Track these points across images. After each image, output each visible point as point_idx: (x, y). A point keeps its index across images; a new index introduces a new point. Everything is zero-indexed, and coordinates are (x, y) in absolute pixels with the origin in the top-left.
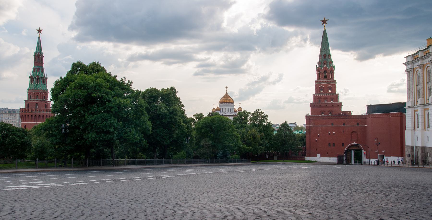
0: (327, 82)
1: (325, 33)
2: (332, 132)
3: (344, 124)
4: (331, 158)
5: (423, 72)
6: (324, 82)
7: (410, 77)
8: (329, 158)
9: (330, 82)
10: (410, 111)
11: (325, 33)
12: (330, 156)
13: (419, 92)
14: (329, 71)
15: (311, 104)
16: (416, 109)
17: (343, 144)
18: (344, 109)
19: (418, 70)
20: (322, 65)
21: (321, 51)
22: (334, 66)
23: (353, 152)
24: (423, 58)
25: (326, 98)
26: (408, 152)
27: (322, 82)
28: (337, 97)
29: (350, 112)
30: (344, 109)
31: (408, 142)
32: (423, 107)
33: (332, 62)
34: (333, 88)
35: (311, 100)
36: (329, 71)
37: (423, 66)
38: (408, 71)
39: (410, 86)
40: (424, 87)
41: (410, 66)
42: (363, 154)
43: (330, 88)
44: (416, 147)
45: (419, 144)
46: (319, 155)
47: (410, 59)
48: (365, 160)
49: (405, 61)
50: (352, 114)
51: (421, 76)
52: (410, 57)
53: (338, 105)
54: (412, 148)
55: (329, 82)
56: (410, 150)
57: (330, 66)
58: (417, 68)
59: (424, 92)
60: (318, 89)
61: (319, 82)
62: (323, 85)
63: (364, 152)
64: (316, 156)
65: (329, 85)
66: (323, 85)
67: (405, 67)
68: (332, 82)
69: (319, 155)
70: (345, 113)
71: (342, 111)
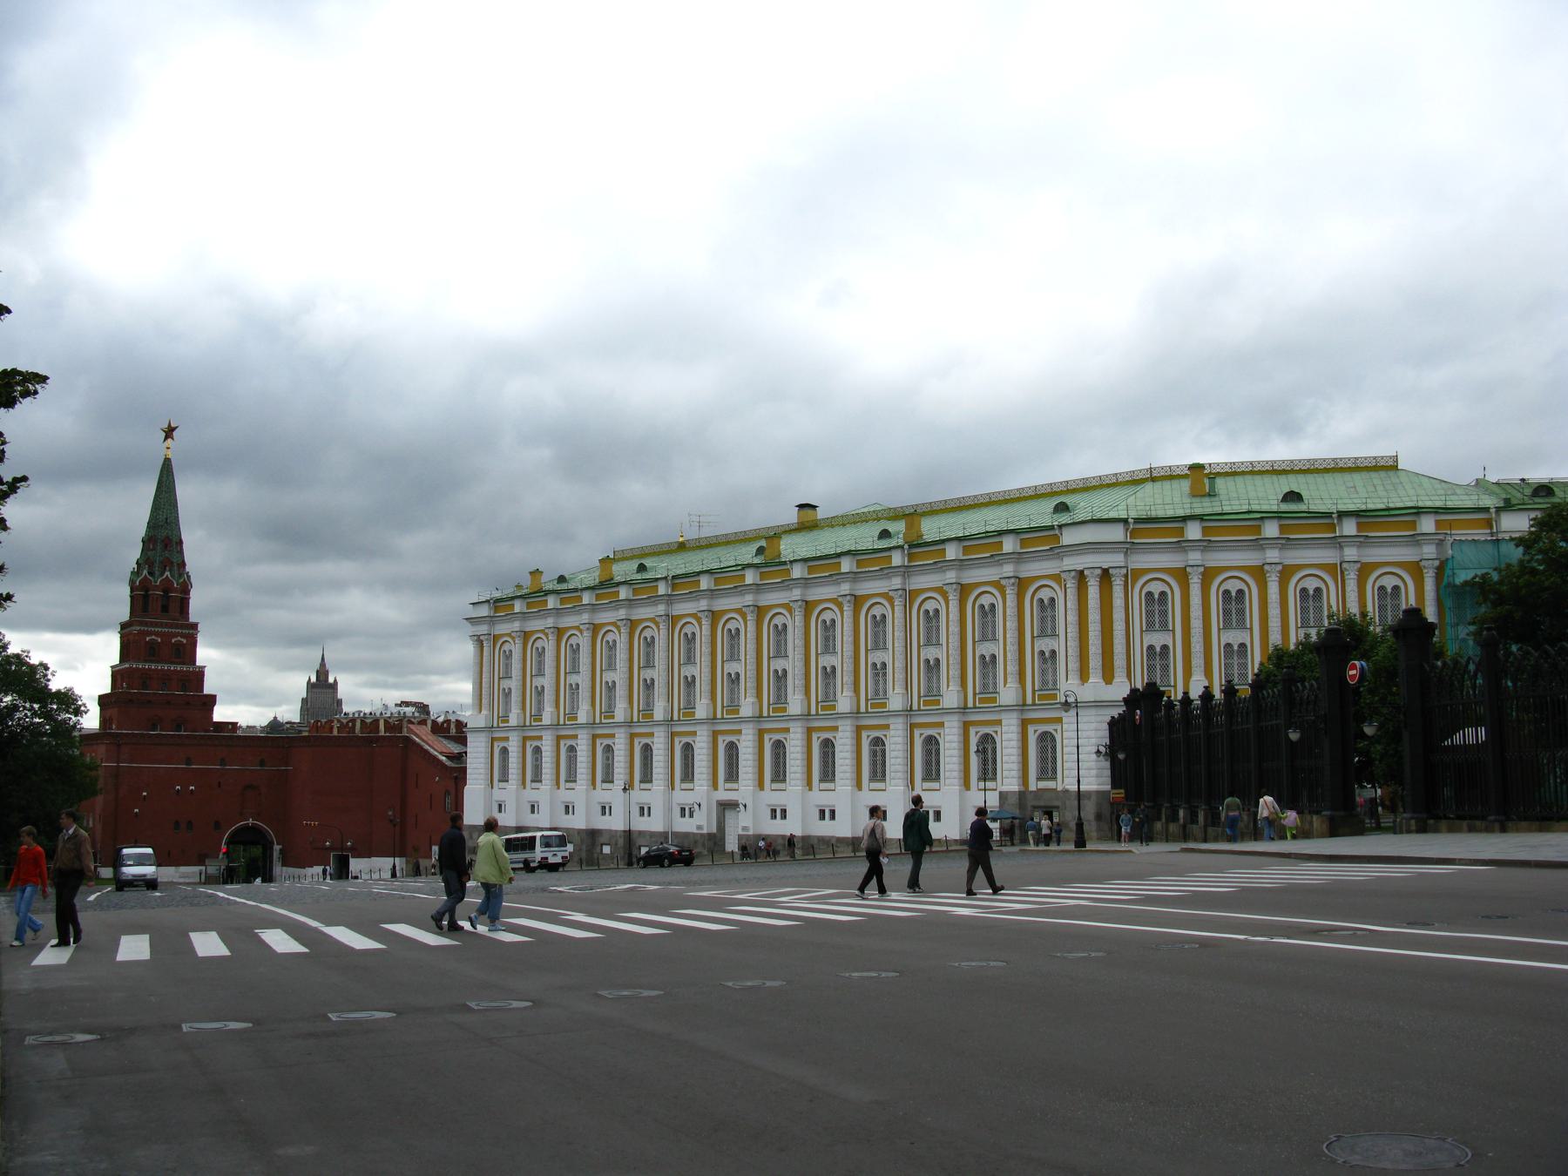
0: (171, 626)
3: (223, 762)
4: (183, 869)
6: (161, 625)
9: (177, 626)
12: (177, 863)
14: (175, 590)
17: (217, 825)
20: (157, 571)
21: (153, 525)
25: (165, 678)
27: (156, 625)
28: (199, 675)
29: (234, 724)
30: (220, 714)
33: (183, 564)
36: (175, 590)
42: (276, 854)
48: (278, 869)
57: (180, 575)
62: (157, 634)
63: (277, 848)
65: (176, 635)
66: (157, 634)
70: (222, 726)
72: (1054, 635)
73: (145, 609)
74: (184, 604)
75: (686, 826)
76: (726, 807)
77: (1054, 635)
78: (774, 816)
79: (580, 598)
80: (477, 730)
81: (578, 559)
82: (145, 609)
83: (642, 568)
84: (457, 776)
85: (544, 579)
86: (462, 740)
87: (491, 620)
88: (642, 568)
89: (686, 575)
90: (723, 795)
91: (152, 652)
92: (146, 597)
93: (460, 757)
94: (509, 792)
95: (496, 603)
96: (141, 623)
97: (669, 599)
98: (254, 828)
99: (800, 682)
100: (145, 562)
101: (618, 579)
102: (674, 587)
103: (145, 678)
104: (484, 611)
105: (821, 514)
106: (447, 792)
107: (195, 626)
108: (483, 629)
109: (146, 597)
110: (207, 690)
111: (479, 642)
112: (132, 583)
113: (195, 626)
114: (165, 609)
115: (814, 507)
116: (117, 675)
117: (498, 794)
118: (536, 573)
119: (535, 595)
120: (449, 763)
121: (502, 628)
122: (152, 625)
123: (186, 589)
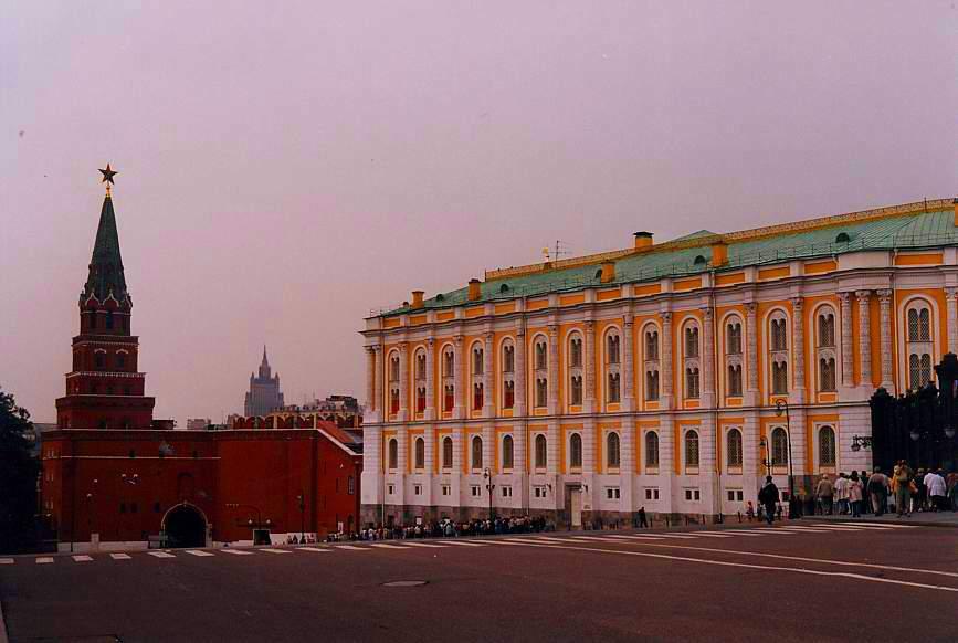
1: (108, 203)
2: (130, 476)
4: (128, 543)
8: (120, 543)
11: (108, 203)
14: (118, 309)
15: (59, 402)
17: (157, 507)
18: (158, 414)
20: (101, 296)
22: (129, 297)
28: (141, 381)
30: (158, 414)
36: (118, 309)
42: (207, 531)
46: (95, 537)
50: (175, 429)
53: (145, 405)
64: (88, 540)
65: (120, 347)
69: (95, 537)
72: (926, 338)
73: (93, 325)
75: (538, 504)
76: (573, 488)
77: (926, 338)
78: (689, 497)
79: (453, 313)
80: (369, 425)
81: (452, 282)
82: (93, 325)
83: (504, 288)
84: (357, 465)
85: (425, 297)
86: (360, 433)
87: (381, 333)
88: (504, 288)
89: (537, 296)
90: (568, 478)
91: (101, 362)
92: (93, 317)
93: (359, 448)
94: (394, 478)
95: (384, 318)
96: (90, 339)
97: (524, 316)
99: (752, 376)
101: (485, 298)
102: (528, 304)
103: (95, 385)
104: (375, 325)
105: (656, 241)
106: (350, 477)
107: (135, 339)
108: (375, 340)
109: (93, 317)
110: (146, 395)
111: (372, 350)
112: (81, 303)
113: (135, 339)
114: (110, 326)
115: (649, 235)
116: (71, 383)
117: (390, 479)
118: (418, 294)
119: (418, 307)
120: (352, 453)
121: (391, 340)
122: (98, 339)
123: (127, 306)
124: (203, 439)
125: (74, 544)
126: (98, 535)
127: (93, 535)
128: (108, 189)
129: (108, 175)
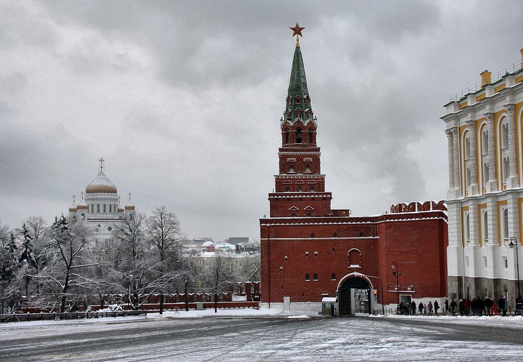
1: (298, 54)
2: (311, 252)
5: (476, 134)
7: (454, 143)
10: (455, 209)
11: (298, 54)
13: (469, 173)
14: (305, 128)
16: (464, 205)
18: (335, 205)
19: (467, 131)
21: (291, 90)
23: (353, 290)
24: (474, 109)
26: (452, 288)
29: (347, 212)
30: (335, 205)
31: (452, 271)
32: (476, 203)
34: (315, 164)
35: (272, 188)
37: (475, 124)
38: (450, 133)
39: (453, 162)
40: (477, 164)
41: (452, 124)
43: (308, 165)
44: (467, 278)
45: (470, 273)
46: (287, 299)
47: (452, 110)
48: (376, 306)
49: (445, 112)
51: (471, 142)
52: (452, 106)
54: (460, 279)
55: (306, 150)
56: (455, 284)
58: (465, 126)
59: (478, 173)
60: (285, 165)
61: (286, 150)
67: (444, 126)
68: (313, 150)
69: (287, 299)
70: (337, 212)
71: (331, 209)
74: (312, 137)
98: (358, 278)
100: (288, 115)
107: (318, 150)
112: (285, 128)
113: (318, 150)
123: (312, 128)
124: (367, 226)
125: (271, 303)
126: (289, 298)
127: (285, 298)
128: (298, 41)
129: (297, 31)
